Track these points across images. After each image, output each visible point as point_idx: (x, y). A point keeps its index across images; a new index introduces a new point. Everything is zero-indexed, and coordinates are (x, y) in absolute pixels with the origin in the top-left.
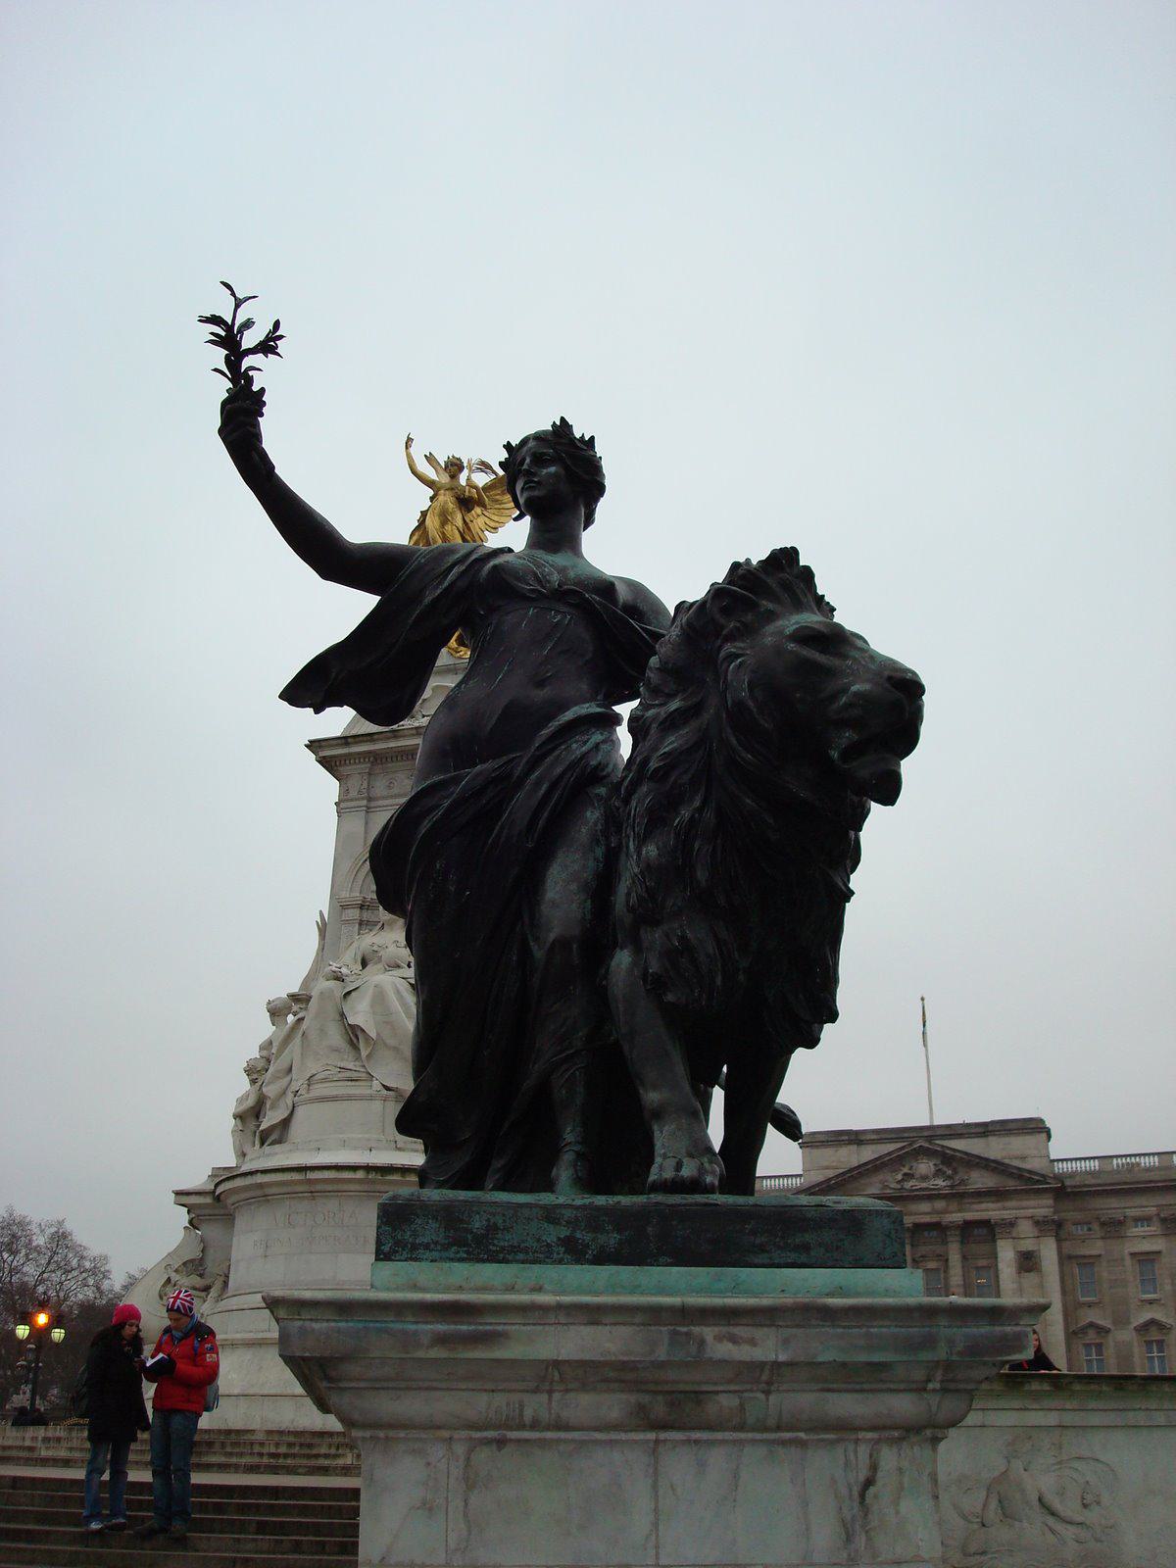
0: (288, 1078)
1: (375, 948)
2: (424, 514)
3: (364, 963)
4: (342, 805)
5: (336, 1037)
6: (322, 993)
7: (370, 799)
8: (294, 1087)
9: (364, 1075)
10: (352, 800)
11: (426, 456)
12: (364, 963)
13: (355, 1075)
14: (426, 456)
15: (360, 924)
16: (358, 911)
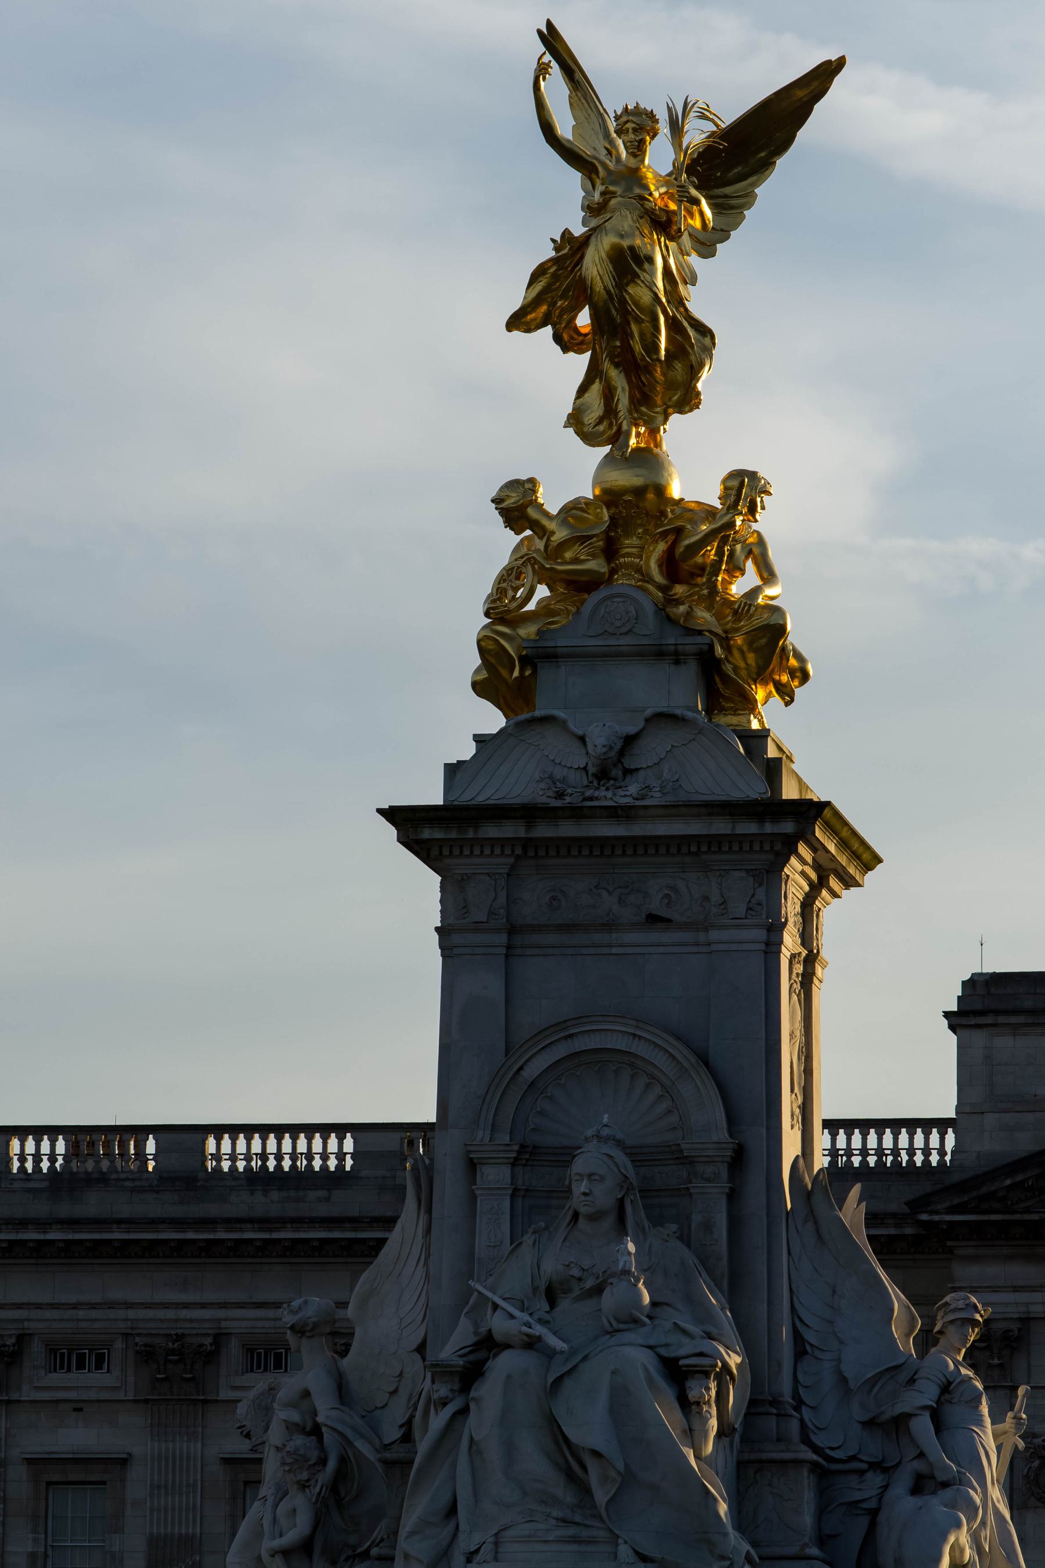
0: (452, 1525)
1: (575, 1272)
2: (571, 249)
3: (551, 1296)
4: (456, 939)
5: (535, 1461)
6: (509, 1377)
7: (512, 930)
8: (466, 1543)
9: (602, 1533)
10: (477, 927)
11: (540, 32)
12: (551, 1296)
13: (585, 1533)
14: (540, 32)
15: (512, 1196)
16: (506, 1172)
